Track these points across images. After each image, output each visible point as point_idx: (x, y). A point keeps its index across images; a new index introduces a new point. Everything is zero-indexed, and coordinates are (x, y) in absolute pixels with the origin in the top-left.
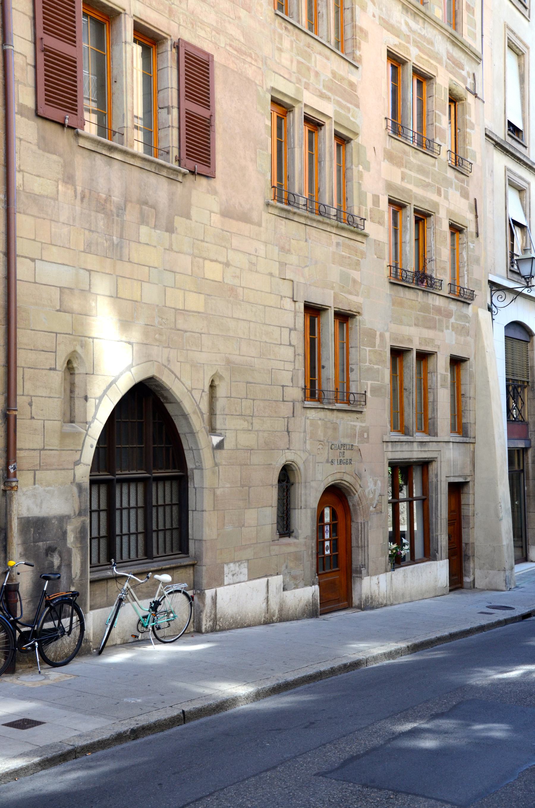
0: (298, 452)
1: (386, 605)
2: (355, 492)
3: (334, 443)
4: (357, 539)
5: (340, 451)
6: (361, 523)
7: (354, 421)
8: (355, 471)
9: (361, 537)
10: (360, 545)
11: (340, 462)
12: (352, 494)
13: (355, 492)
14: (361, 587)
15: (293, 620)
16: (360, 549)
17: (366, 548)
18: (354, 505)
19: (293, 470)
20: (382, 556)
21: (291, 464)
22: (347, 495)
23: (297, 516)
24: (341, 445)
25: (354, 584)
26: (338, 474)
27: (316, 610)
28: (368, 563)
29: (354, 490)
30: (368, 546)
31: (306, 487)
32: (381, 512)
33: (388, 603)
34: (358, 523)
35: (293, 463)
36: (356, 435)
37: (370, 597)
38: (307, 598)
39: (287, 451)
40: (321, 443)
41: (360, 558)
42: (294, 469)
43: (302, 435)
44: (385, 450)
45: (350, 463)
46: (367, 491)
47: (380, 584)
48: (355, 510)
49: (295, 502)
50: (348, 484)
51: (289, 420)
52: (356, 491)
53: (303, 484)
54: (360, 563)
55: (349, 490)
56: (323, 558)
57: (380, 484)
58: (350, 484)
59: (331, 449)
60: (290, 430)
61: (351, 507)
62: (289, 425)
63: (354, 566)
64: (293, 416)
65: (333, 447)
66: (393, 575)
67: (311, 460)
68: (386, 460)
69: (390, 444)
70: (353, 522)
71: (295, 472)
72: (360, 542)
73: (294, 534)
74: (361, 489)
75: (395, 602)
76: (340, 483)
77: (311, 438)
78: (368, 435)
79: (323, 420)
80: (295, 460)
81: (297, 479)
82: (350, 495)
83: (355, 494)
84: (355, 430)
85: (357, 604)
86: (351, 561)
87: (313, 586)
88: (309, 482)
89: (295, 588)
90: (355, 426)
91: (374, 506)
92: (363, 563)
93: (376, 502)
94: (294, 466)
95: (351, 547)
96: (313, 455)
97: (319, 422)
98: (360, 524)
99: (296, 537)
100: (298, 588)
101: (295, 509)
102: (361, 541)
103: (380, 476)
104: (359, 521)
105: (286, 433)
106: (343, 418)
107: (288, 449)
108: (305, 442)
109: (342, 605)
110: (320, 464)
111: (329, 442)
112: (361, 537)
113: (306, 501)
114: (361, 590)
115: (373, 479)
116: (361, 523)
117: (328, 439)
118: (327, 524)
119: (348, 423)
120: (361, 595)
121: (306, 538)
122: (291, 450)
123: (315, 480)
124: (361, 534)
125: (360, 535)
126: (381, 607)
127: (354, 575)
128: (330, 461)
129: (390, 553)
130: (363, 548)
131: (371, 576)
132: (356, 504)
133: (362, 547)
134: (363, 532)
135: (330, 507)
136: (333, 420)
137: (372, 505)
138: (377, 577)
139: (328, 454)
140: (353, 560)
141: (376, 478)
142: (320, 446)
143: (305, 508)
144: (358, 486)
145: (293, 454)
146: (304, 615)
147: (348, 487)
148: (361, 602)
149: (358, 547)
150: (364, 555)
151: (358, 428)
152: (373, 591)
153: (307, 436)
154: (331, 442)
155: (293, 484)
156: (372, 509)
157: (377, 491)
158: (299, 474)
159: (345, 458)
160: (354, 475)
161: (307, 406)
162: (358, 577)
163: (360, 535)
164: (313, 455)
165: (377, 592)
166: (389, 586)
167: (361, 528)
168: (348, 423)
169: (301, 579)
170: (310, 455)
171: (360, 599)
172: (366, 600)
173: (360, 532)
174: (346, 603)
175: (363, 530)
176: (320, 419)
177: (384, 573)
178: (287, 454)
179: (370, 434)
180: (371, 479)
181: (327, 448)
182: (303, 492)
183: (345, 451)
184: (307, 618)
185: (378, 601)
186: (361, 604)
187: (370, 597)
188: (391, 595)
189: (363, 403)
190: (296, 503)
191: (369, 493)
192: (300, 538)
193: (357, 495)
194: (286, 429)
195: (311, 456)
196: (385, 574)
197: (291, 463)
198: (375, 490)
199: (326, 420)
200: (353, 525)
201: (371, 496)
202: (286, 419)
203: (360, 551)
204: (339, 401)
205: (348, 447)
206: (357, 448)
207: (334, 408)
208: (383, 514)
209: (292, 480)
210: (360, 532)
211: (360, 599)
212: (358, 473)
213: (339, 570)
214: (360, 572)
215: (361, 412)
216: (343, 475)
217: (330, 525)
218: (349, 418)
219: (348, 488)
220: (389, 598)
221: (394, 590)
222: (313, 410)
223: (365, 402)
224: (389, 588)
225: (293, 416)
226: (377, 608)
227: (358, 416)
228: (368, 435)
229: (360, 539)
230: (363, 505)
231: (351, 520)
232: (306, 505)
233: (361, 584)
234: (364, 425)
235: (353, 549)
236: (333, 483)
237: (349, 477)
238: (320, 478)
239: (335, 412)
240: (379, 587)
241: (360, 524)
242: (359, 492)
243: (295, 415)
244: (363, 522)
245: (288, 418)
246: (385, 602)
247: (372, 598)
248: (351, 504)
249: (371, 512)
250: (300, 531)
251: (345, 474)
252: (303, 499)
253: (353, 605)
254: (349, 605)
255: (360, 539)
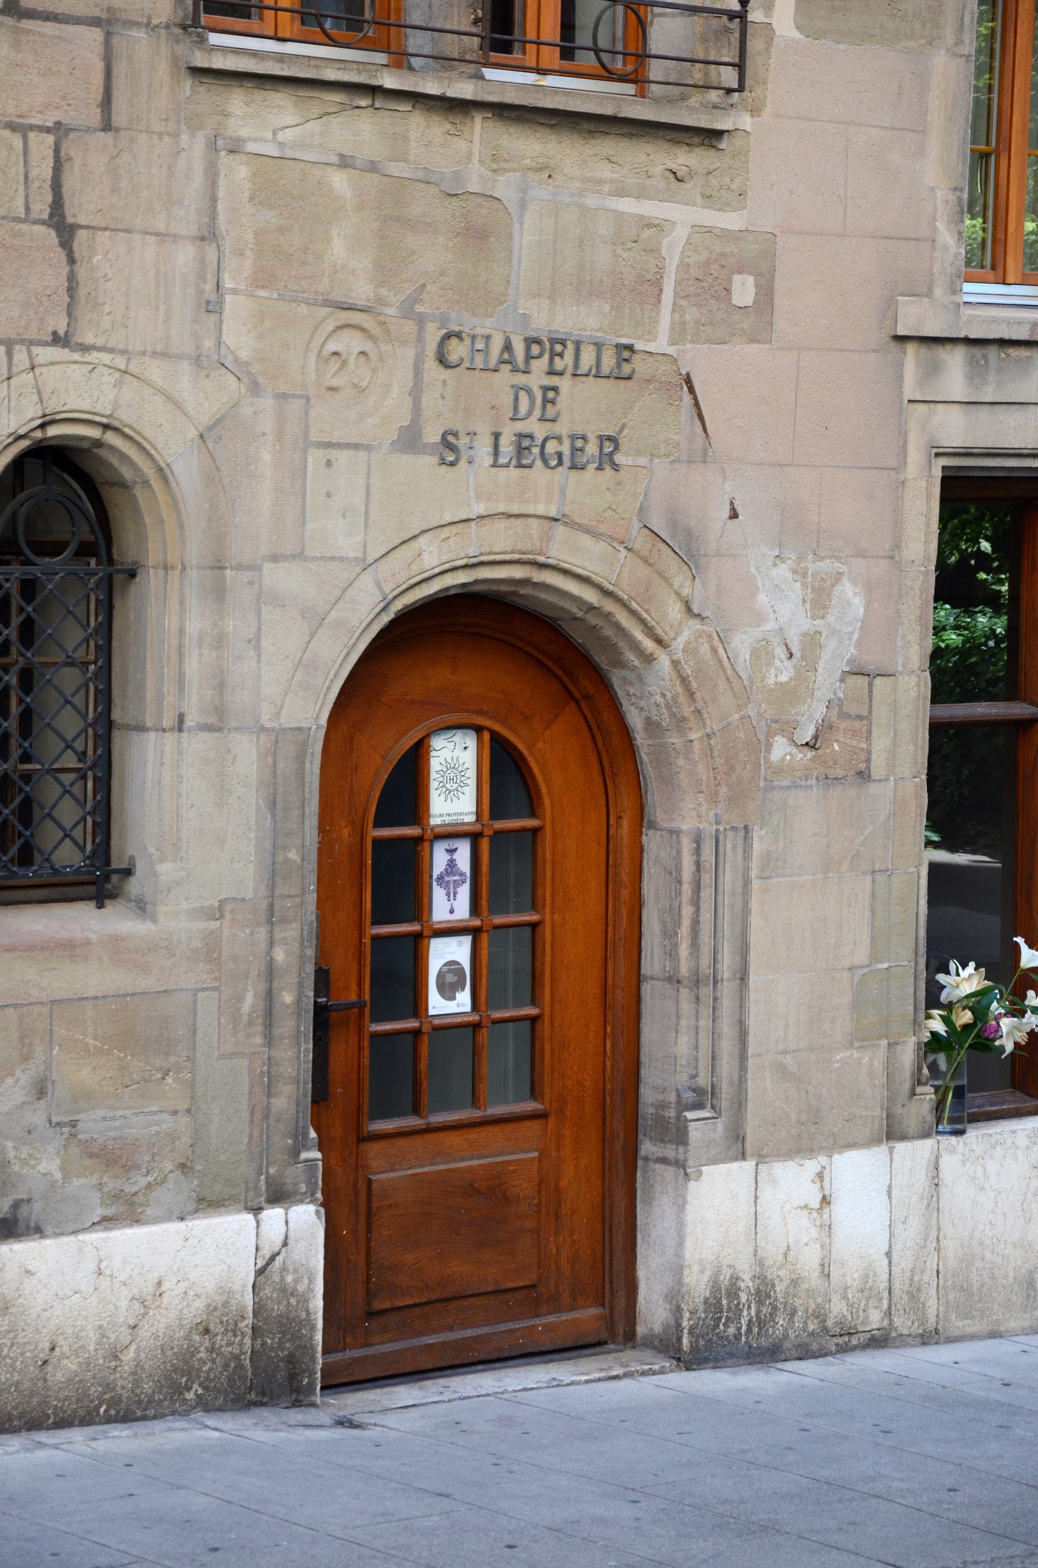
0: (155, 371)
1: (879, 1341)
2: (649, 645)
3: (469, 323)
4: (670, 934)
5: (520, 379)
6: (698, 841)
7: (641, 194)
8: (642, 511)
9: (696, 923)
10: (684, 971)
11: (521, 450)
12: (630, 656)
13: (649, 645)
14: (681, 1224)
15: (87, 1420)
16: (684, 992)
17: (727, 991)
18: (651, 725)
19: (123, 485)
20: (860, 1038)
21: (98, 443)
22: (602, 660)
23: (149, 772)
24: (531, 341)
25: (648, 1202)
26: (502, 524)
27: (291, 1360)
28: (742, 1080)
29: (638, 635)
30: (743, 978)
31: (219, 594)
32: (864, 776)
33: (902, 1324)
34: (676, 833)
35: (111, 438)
36: (658, 284)
37: (747, 1282)
38: (209, 1285)
39: (45, 354)
40: (356, 317)
41: (683, 1046)
42: (127, 474)
43: (185, 256)
44: (910, 391)
45: (607, 461)
46: (742, 644)
47: (840, 1209)
48: (663, 755)
49: (141, 687)
50: (590, 596)
51: (69, 148)
52: (659, 641)
53: (193, 574)
54: (682, 1079)
55: (608, 632)
56: (417, 1033)
57: (858, 606)
58: (607, 593)
59: (442, 361)
60: (77, 212)
61: (640, 738)
62: (70, 182)
63: (648, 1095)
64: (107, 126)
65: (457, 350)
66: (945, 1161)
67: (267, 424)
68: (915, 457)
69: (955, 359)
70: (652, 825)
71: (138, 492)
72: (684, 951)
73: (134, 886)
74: (695, 625)
75: (958, 1325)
76: (526, 582)
77: (262, 279)
78: (766, 293)
79: (373, 167)
80: (125, 416)
81: (153, 545)
82: (620, 663)
83: (649, 659)
84: (654, 251)
85: (657, 1328)
86: (637, 1064)
87: (274, 1215)
88: (254, 567)
89: (107, 1222)
90: (659, 227)
91: (807, 736)
92: (703, 1080)
93: (819, 711)
94: (124, 457)
95: (637, 979)
96: (282, 397)
97: (339, 181)
98: (687, 846)
99: (142, 908)
100: (137, 1221)
101: (142, 728)
102: (695, 944)
103: (861, 554)
104: (687, 825)
105: (50, 236)
106: (547, 171)
107: (58, 340)
108: (213, 307)
109: (549, 1328)
110: (343, 457)
111: (421, 321)
112: (696, 923)
113: (221, 686)
114: (681, 1244)
115: (800, 573)
116: (698, 841)
117: (415, 299)
118: (451, 834)
119: (592, 201)
120: (678, 1269)
121: (217, 913)
122: (85, 348)
123: (299, 556)
124: (696, 904)
125: (687, 911)
126: (844, 1349)
127: (647, 1147)
128: (432, 436)
129: (938, 1026)
130: (706, 991)
131: (762, 1158)
132: (666, 721)
133: (697, 981)
134: (707, 893)
135: (478, 730)
136: (457, 176)
137: (789, 728)
138: (811, 1166)
139: (416, 393)
140: (644, 1058)
141: (826, 566)
142: (350, 343)
143: (208, 728)
144: (674, 611)
145: (108, 378)
146: (179, 1390)
147: (592, 608)
148: (678, 1310)
149: (674, 980)
150: (715, 1036)
151: (681, 234)
152: (772, 1252)
153: (230, 263)
154: (444, 321)
155: (132, 575)
156: (780, 750)
157: (830, 646)
158: (165, 511)
159: (562, 428)
160: (641, 541)
161: (219, 62)
162: (664, 1161)
163: (687, 911)
164: (282, 397)
165: (809, 1259)
166: (915, 1225)
167: (698, 865)
168: (592, 201)
169: (169, 1166)
170: (255, 388)
171: (675, 1297)
172: (713, 1305)
173: (687, 889)
174: (593, 1311)
175: (707, 879)
176: (345, 162)
177: (874, 1141)
178: (50, 377)
179: (780, 286)
180: (782, 572)
181: (410, 353)
182: (194, 626)
183: (564, 384)
184: (205, 1405)
185: (820, 1315)
186: (679, 1326)
187: (747, 1282)
188: (929, 1277)
189: (729, 77)
190: (150, 693)
191: (761, 652)
192: (162, 909)
193: (664, 661)
194: (42, 207)
195: (268, 402)
196: (884, 1148)
197: (94, 433)
198: (812, 642)
199: (396, 169)
200: (651, 841)
201: (781, 672)
202: (42, 145)
203: (686, 1006)
204: (586, 59)
205: (587, 358)
206: (665, 367)
207: (465, 90)
208: (873, 788)
209: (126, 548)
210: (687, 889)
211: (675, 1297)
212: (673, 524)
213: (542, 1116)
214: (681, 1137)
215: (711, 137)
216: (547, 537)
217: (475, 838)
218: (605, 172)
219: (593, 620)
220: (914, 1294)
221: (950, 1247)
222: (281, 98)
223: (740, 66)
224: (911, 1233)
225: (107, 126)
226: (805, 1353)
227: (684, 158)
228: (766, 293)
229: (685, 930)
230: (713, 724)
231: (640, 818)
232: (220, 711)
233: (681, 1207)
234: (732, 221)
235: (646, 988)
236: (462, 578)
237: (599, 547)
238: (348, 545)
239: (479, 124)
240: (828, 1228)
241: (687, 846)
242: (679, 644)
243: (120, 115)
244: (708, 828)
245: (59, 130)
246: (875, 1319)
247: (762, 1294)
248: (635, 720)
249: (779, 770)
250: (166, 870)
251: (560, 530)
252: (194, 666)
253: (641, 1330)
254: (611, 1329)
255: (685, 930)
